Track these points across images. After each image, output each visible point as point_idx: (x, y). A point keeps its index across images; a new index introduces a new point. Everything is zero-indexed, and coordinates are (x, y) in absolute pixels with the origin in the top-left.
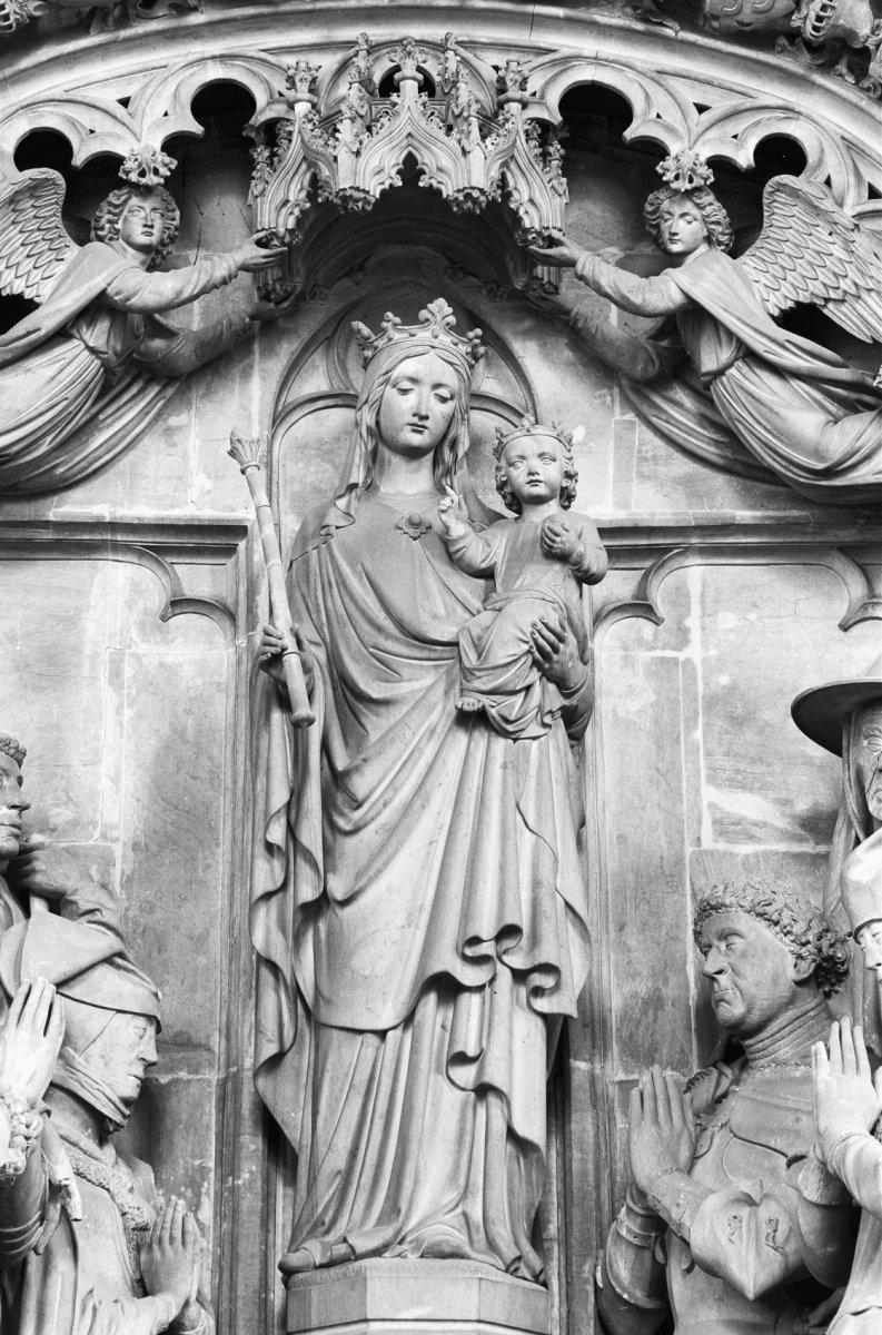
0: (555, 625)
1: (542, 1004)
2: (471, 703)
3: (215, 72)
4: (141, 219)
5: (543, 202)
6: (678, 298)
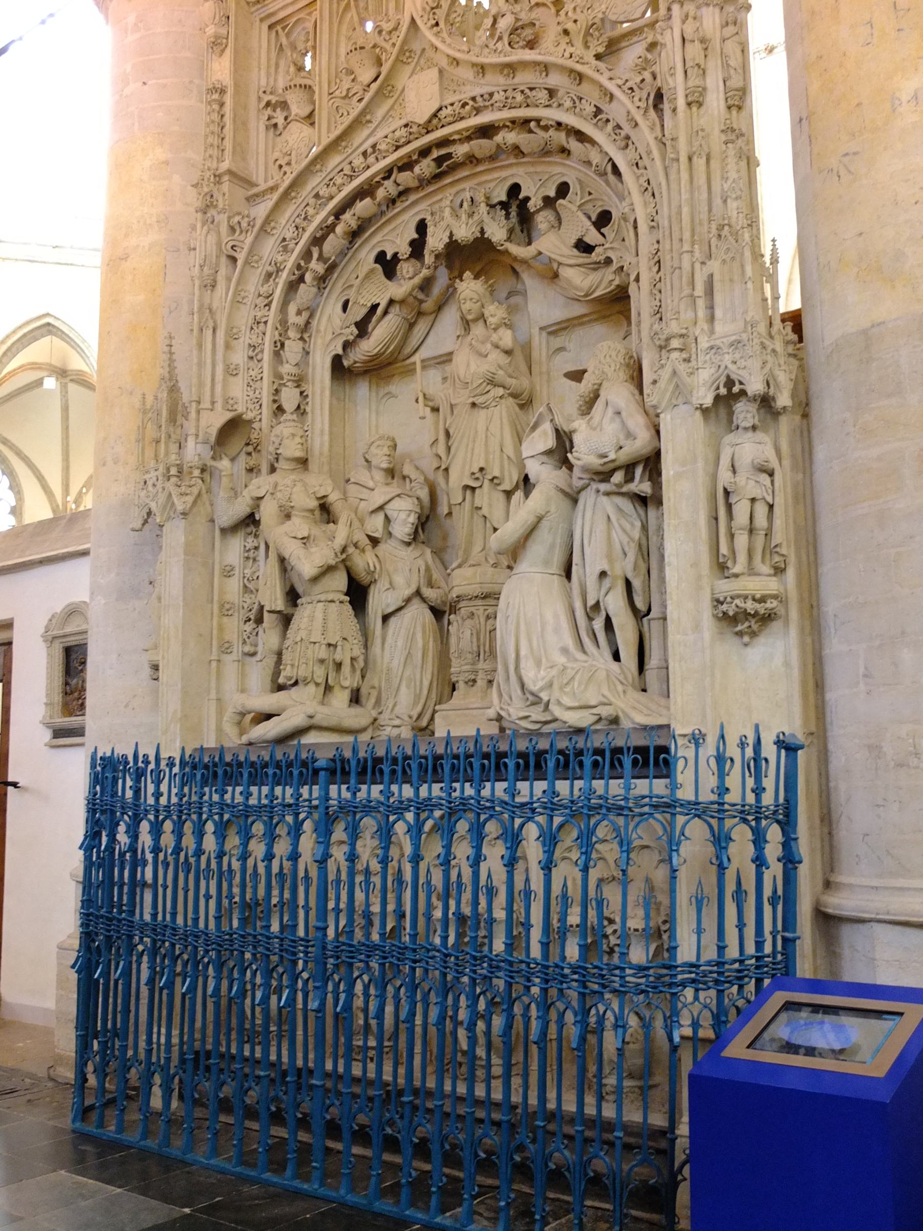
0: (493, 371)
1: (502, 488)
2: (471, 400)
3: (418, 218)
4: (405, 268)
5: (497, 231)
6: (535, 252)
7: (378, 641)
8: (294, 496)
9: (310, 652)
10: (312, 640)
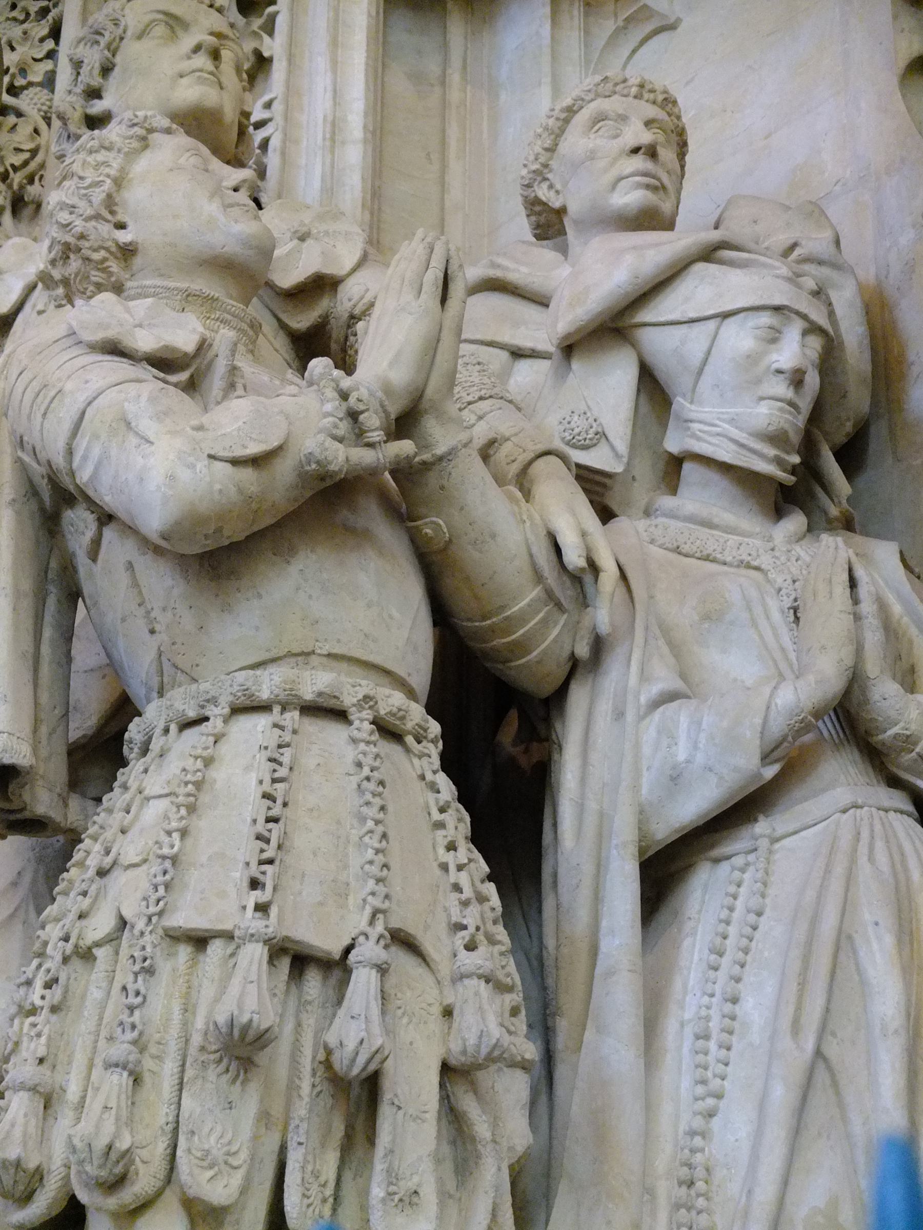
7: (618, 996)
8: (136, 196)
9: (162, 1002)
10: (185, 918)
